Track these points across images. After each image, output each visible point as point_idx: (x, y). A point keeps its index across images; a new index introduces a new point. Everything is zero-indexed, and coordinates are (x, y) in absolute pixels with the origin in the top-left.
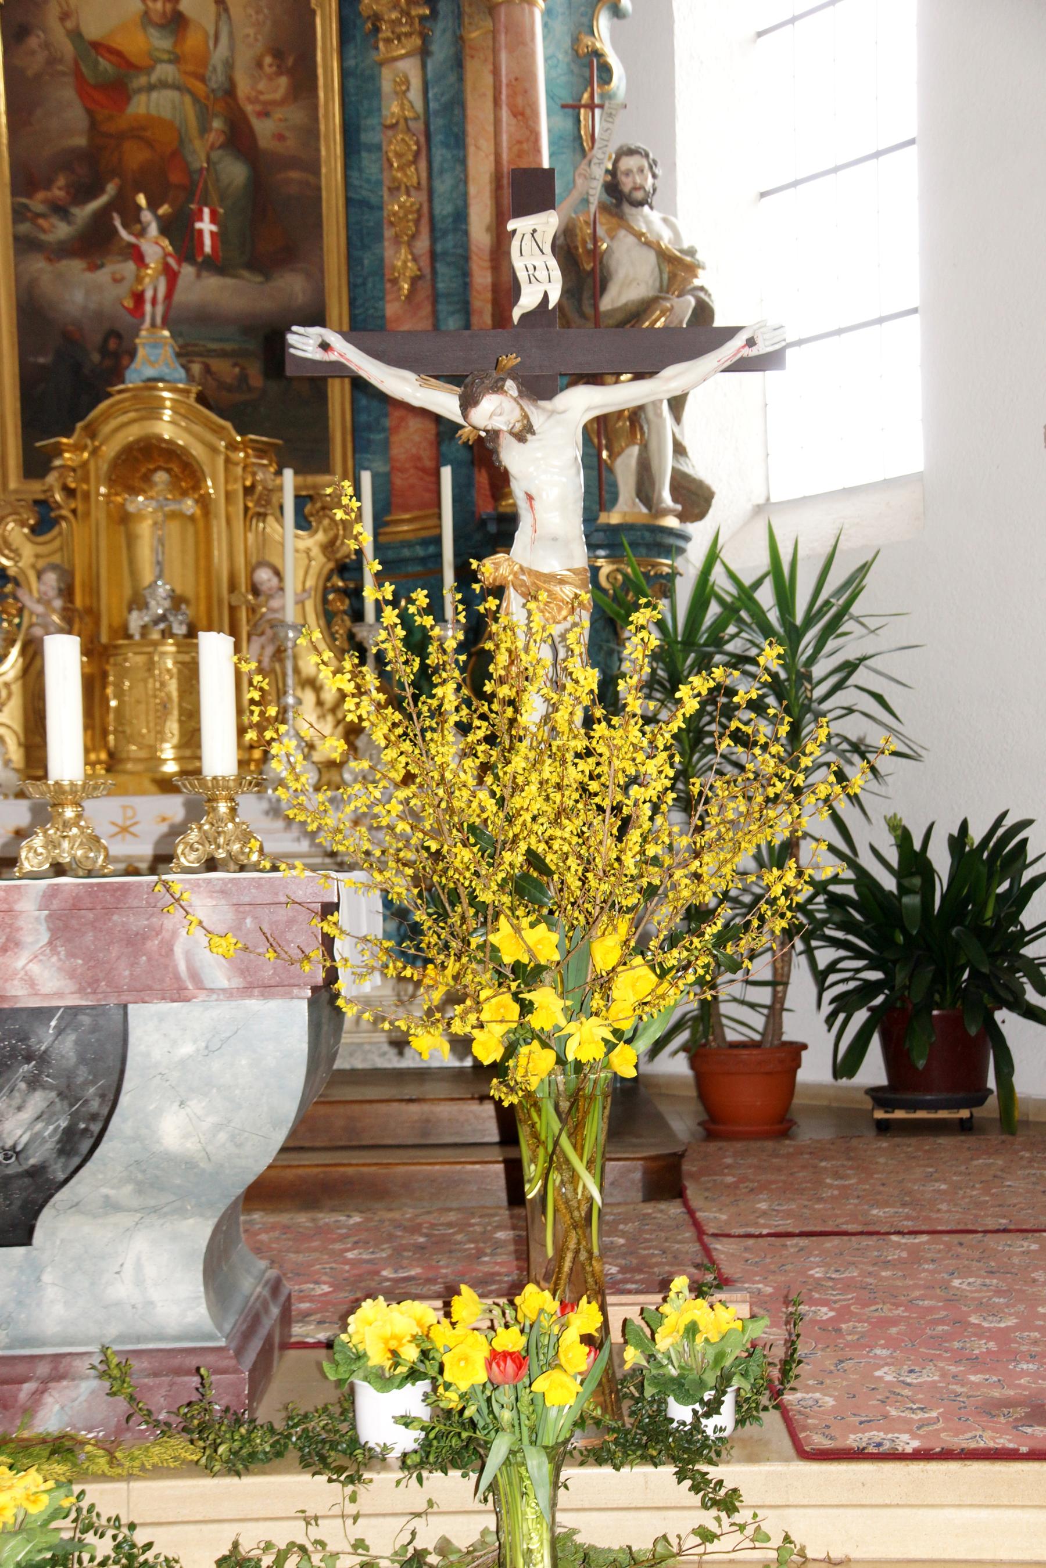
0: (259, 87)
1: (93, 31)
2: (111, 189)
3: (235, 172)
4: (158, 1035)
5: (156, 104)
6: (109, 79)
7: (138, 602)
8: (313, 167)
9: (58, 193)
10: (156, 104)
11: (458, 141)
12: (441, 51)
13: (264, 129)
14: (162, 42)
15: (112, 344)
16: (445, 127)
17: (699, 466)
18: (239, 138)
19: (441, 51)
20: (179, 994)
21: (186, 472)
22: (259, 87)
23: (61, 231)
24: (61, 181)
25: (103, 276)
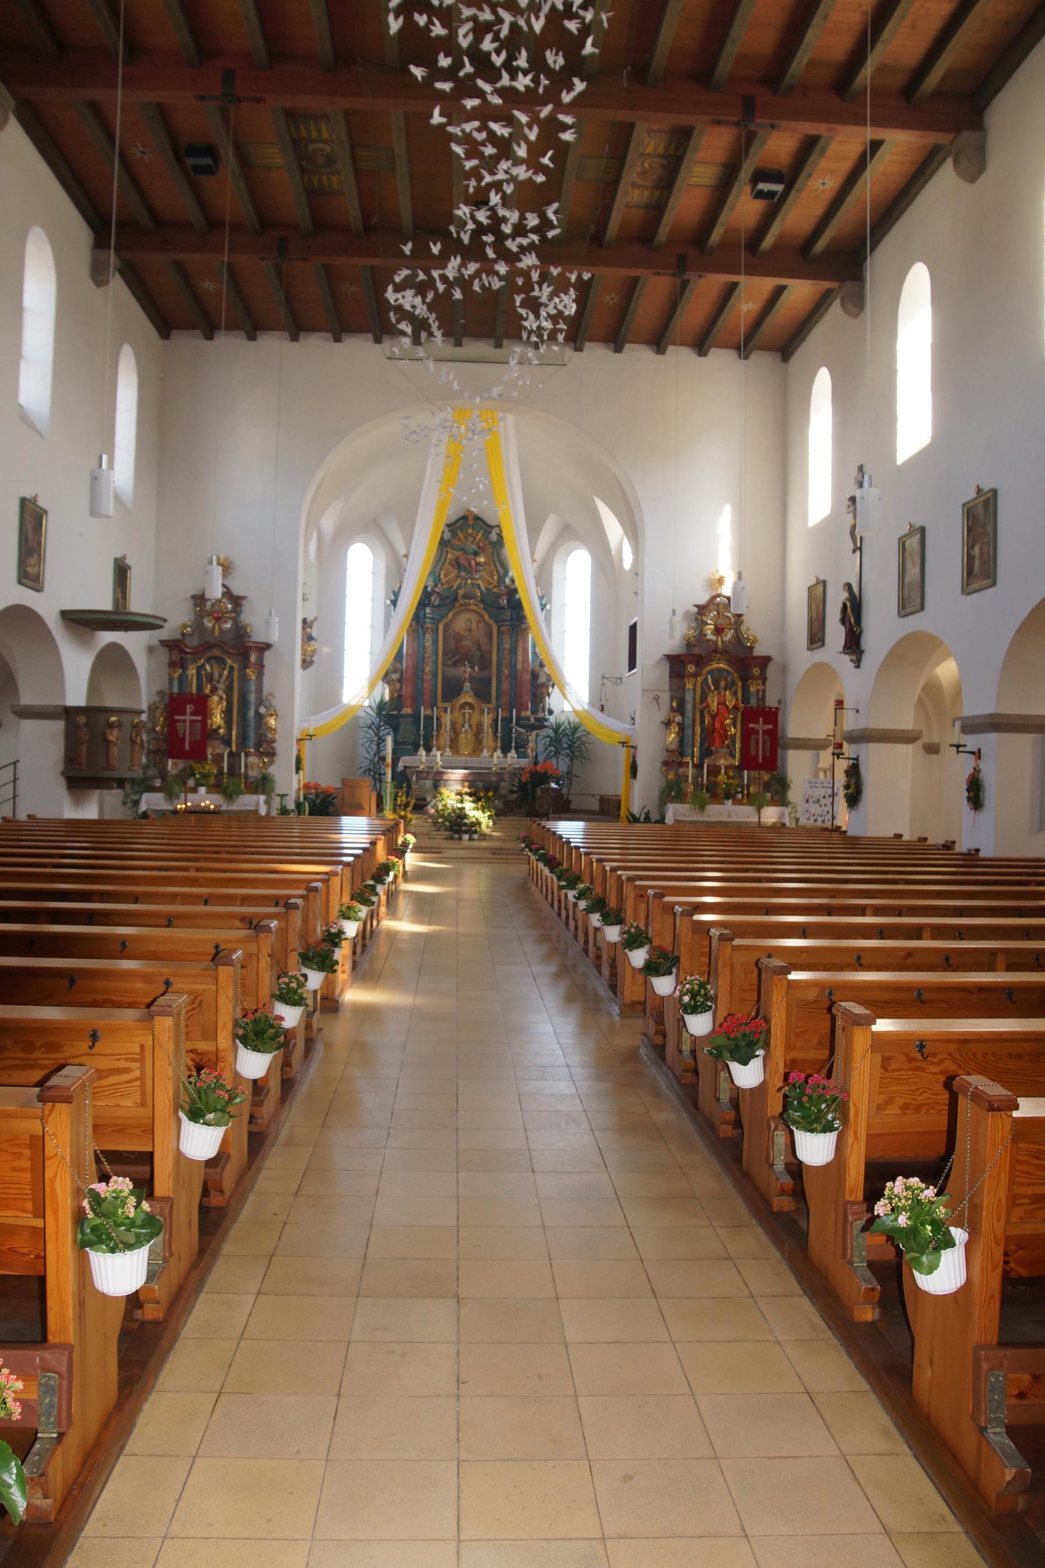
0: (482, 640)
3: (478, 654)
4: (503, 784)
5: (466, 643)
6: (459, 638)
7: (463, 726)
8: (491, 654)
10: (466, 643)
11: (516, 653)
12: (514, 639)
13: (484, 647)
14: (467, 633)
16: (513, 651)
17: (552, 707)
18: (479, 648)
19: (514, 639)
20: (504, 781)
21: (470, 706)
22: (482, 640)
23: (450, 662)
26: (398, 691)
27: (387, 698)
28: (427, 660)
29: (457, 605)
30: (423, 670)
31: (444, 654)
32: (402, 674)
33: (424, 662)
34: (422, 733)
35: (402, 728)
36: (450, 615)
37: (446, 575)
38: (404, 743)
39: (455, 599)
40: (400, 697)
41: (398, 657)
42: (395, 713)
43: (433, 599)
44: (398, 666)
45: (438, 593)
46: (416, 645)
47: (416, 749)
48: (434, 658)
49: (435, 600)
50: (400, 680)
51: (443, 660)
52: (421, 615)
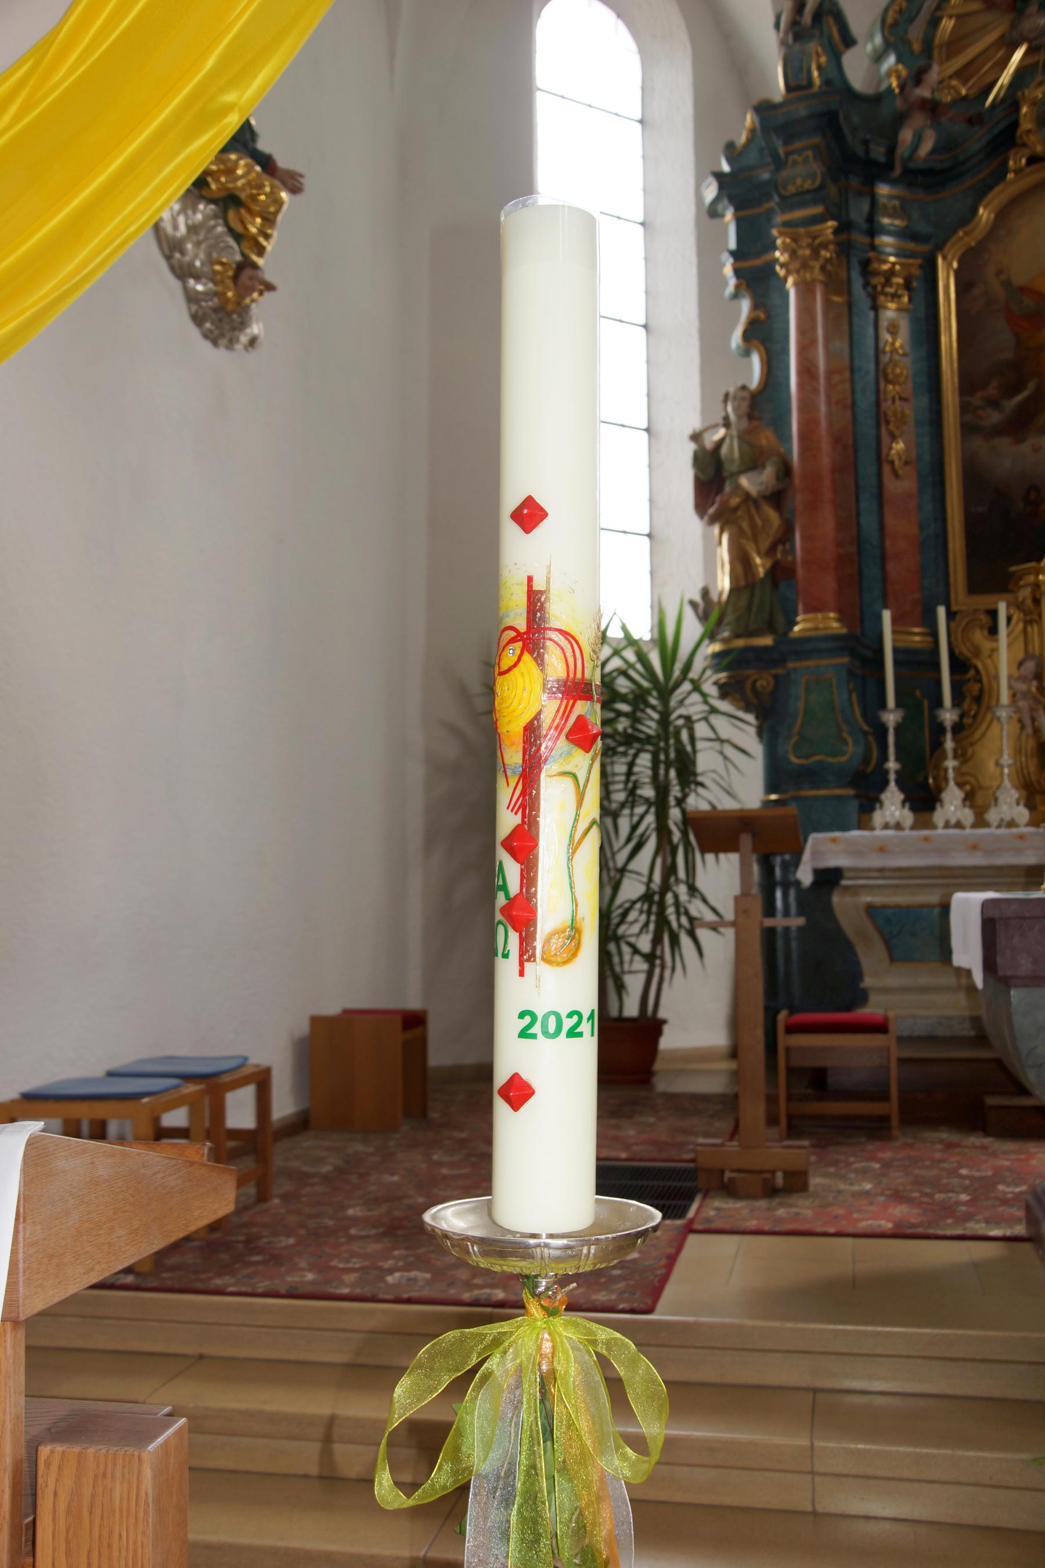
1: (1020, 278)
2: (1031, 386)
9: (992, 391)
15: (1033, 496)
23: (994, 417)
24: (995, 383)
25: (1025, 447)
26: (771, 551)
27: (724, 583)
28: (887, 405)
29: (1016, 161)
30: (880, 458)
31: (968, 385)
32: (785, 471)
33: (880, 418)
34: (891, 718)
35: (799, 700)
36: (984, 214)
37: (954, 46)
38: (811, 776)
39: (1007, 138)
40: (780, 573)
41: (761, 406)
42: (767, 641)
43: (906, 135)
44: (766, 438)
45: (932, 108)
46: (841, 345)
47: (869, 803)
48: (924, 401)
49: (917, 140)
50: (776, 498)
51: (964, 408)
52: (858, 211)
